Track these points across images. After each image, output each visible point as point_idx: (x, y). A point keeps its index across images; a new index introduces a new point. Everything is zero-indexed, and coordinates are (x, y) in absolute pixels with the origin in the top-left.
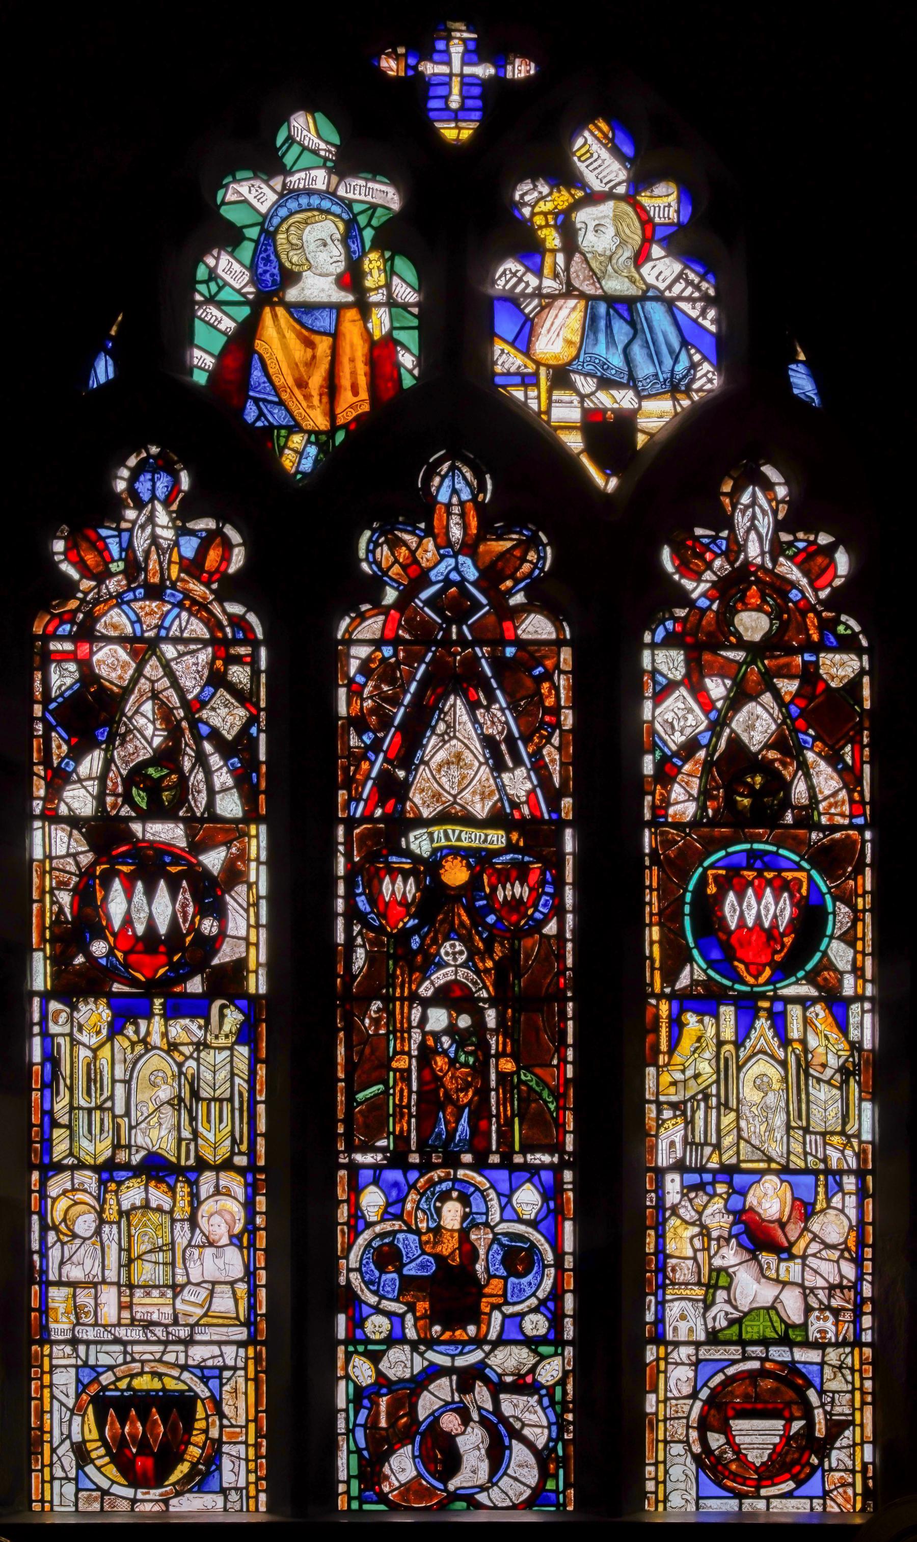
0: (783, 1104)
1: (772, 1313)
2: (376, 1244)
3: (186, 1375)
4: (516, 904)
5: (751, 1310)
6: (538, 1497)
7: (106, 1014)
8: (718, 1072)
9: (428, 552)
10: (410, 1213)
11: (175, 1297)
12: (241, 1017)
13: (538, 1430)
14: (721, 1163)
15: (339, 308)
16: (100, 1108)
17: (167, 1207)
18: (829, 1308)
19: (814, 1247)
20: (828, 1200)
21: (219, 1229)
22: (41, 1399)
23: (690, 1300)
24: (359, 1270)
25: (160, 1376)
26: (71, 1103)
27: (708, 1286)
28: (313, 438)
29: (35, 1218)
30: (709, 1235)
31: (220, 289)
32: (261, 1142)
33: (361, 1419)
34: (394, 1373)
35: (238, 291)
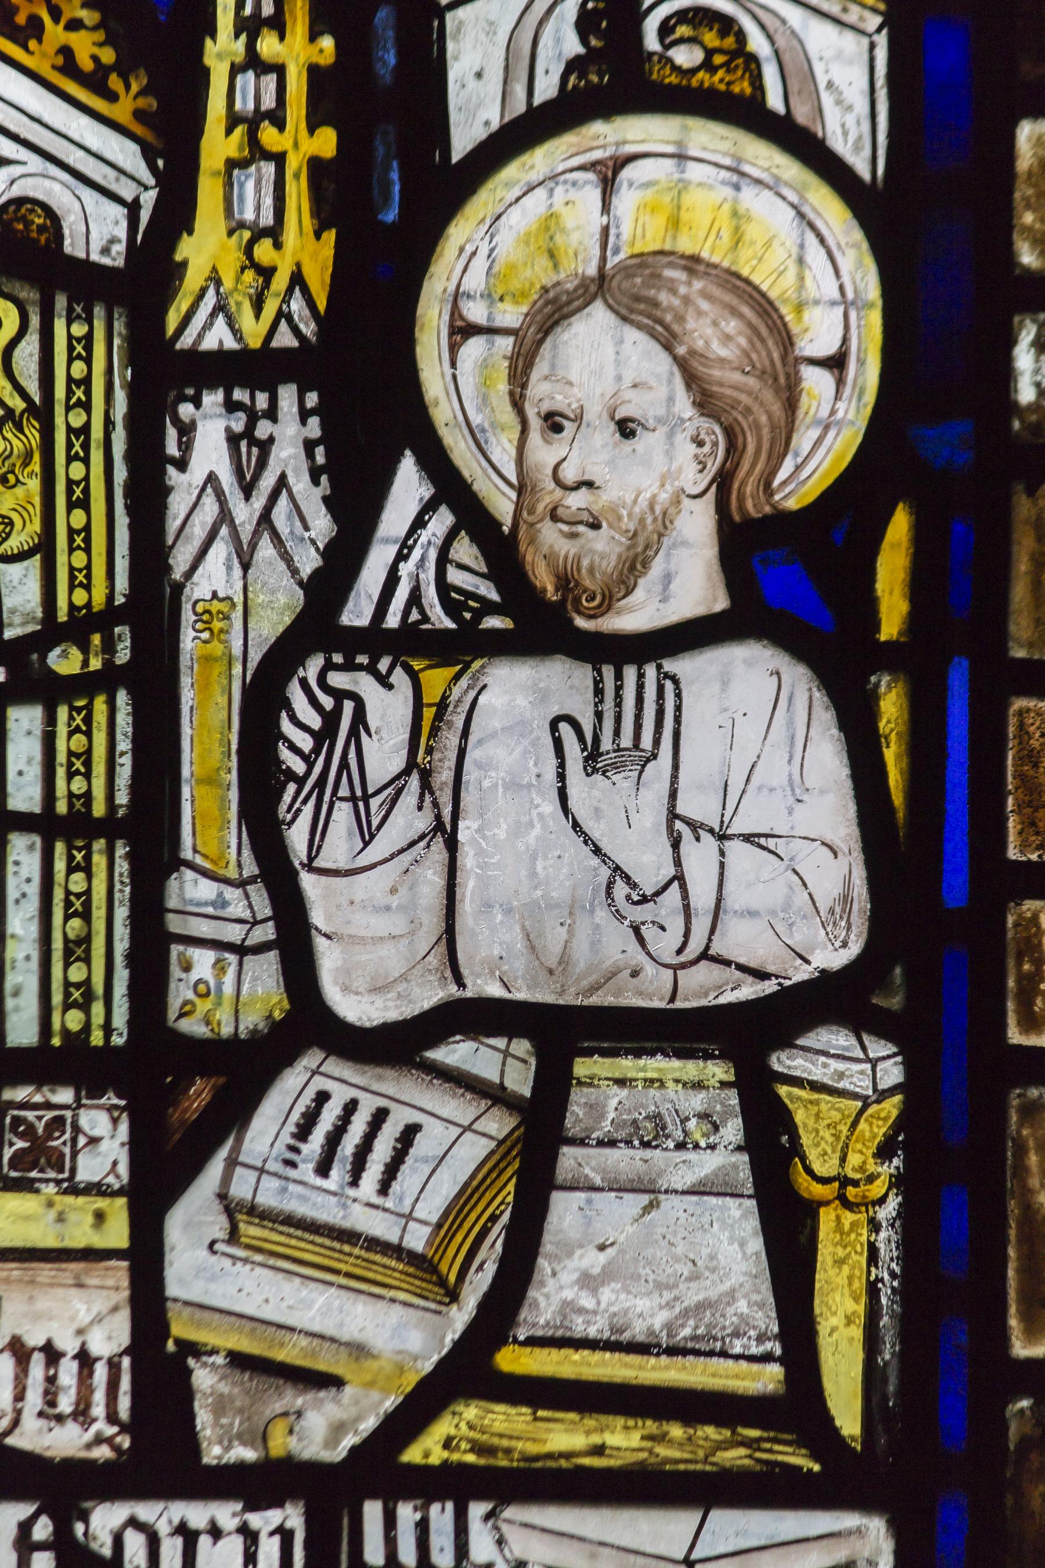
11: (153, 1186)
17: (97, 231)
21: (631, 475)
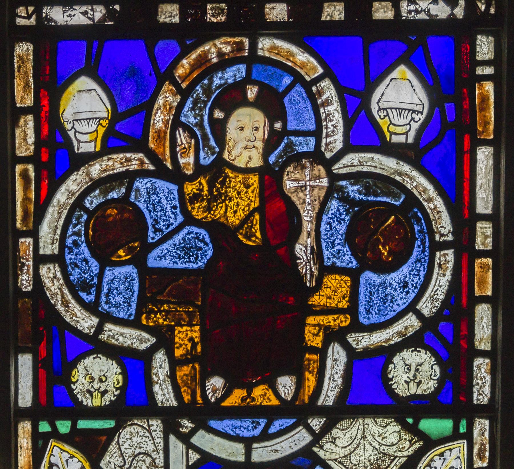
2: (93, 201)
10: (160, 136)
24: (58, 259)
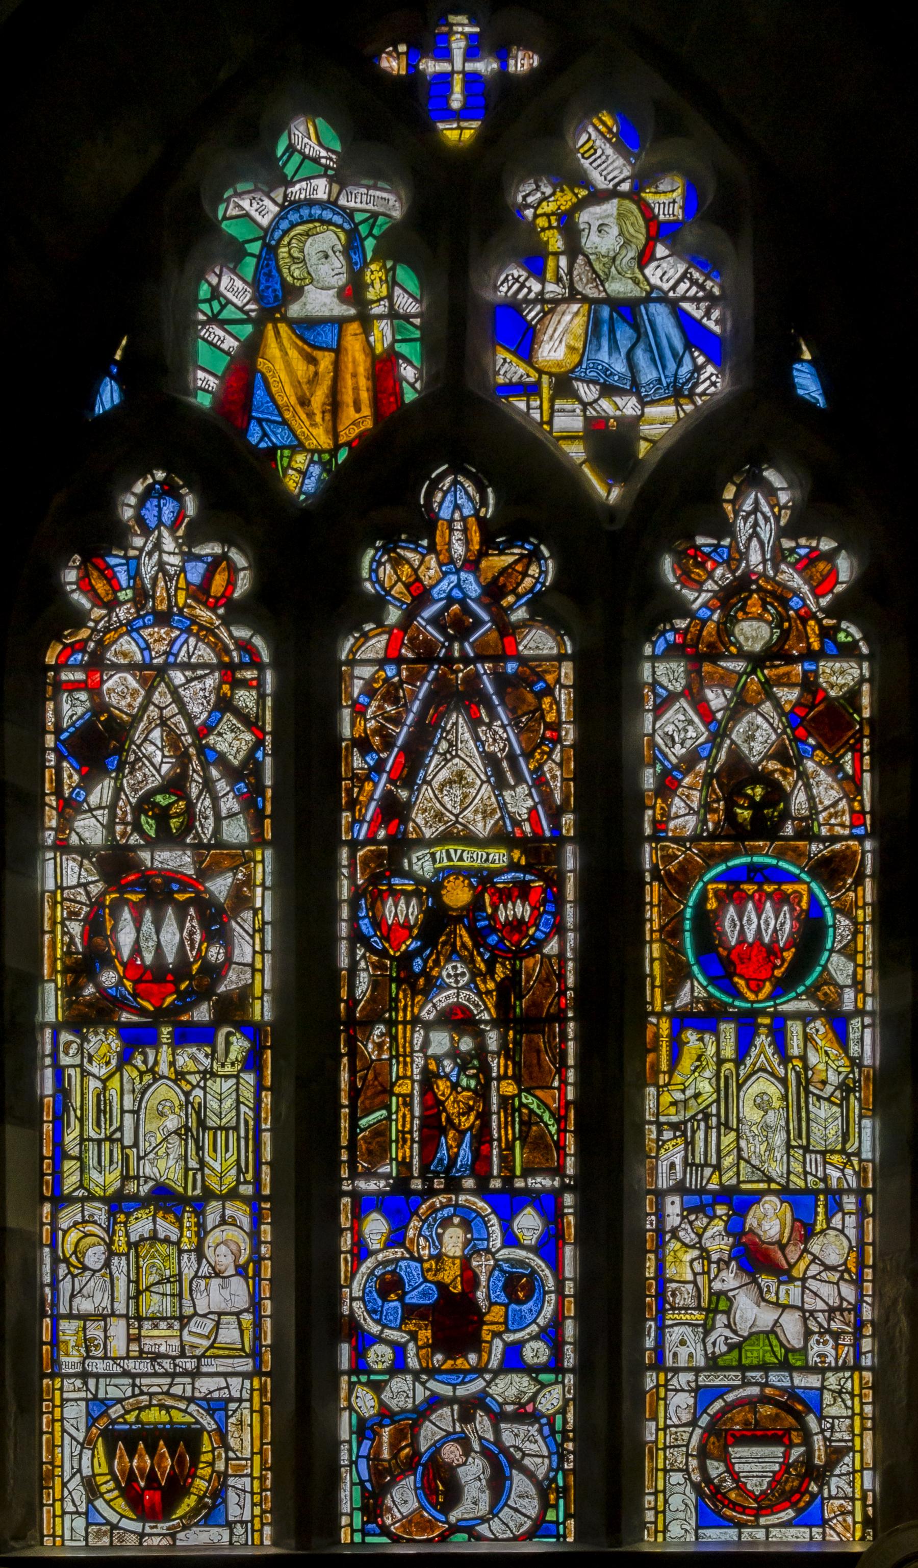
0: (783, 1123)
1: (772, 1337)
2: (378, 1272)
3: (193, 1408)
4: (518, 925)
5: (751, 1334)
6: (539, 1528)
7: (116, 1044)
8: (718, 1091)
9: (431, 570)
10: (412, 1241)
11: (181, 1330)
12: (247, 1044)
13: (539, 1460)
14: (721, 1184)
15: (340, 322)
16: (110, 1139)
17: (174, 1238)
18: (828, 1331)
19: (814, 1269)
20: (828, 1220)
21: (224, 1260)
22: (52, 1433)
23: (690, 1325)
24: (362, 1299)
25: (168, 1408)
26: (81, 1135)
27: (708, 1310)
28: (316, 458)
29: (47, 1250)
30: (708, 1258)
31: (223, 307)
32: (266, 1170)
33: (364, 1451)
34: (395, 1405)
35: (241, 309)
